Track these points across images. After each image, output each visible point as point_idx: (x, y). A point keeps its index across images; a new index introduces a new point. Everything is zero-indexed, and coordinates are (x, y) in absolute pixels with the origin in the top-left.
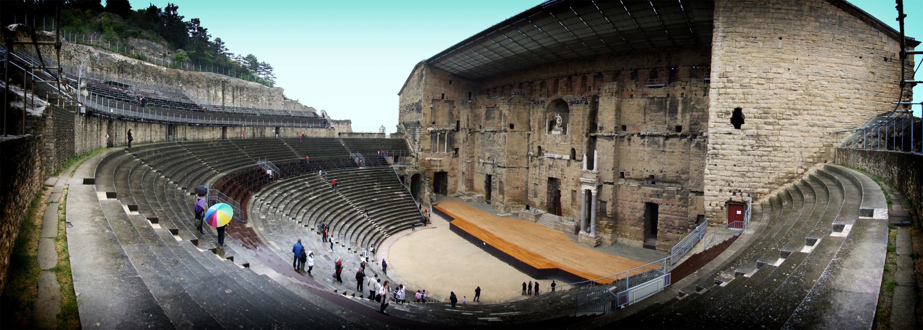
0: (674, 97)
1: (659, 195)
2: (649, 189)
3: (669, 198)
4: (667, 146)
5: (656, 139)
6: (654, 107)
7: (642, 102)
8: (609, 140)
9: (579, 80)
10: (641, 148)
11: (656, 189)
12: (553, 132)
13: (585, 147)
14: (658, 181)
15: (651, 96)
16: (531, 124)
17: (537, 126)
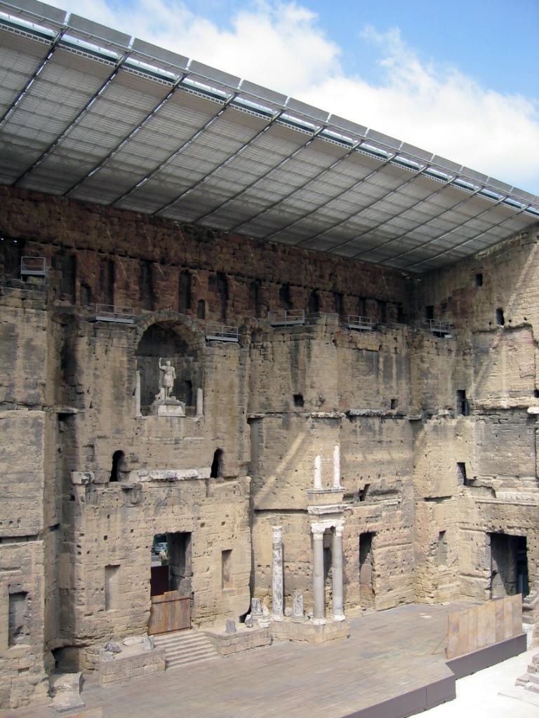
0: (388, 351)
1: (375, 517)
2: (364, 509)
3: (390, 518)
4: (384, 431)
5: (370, 421)
6: (362, 366)
7: (349, 354)
8: (332, 426)
9: (175, 277)
10: (352, 438)
11: (373, 507)
12: (162, 410)
13: (246, 442)
14: (375, 493)
15: (360, 346)
16: (86, 380)
17: (107, 394)
